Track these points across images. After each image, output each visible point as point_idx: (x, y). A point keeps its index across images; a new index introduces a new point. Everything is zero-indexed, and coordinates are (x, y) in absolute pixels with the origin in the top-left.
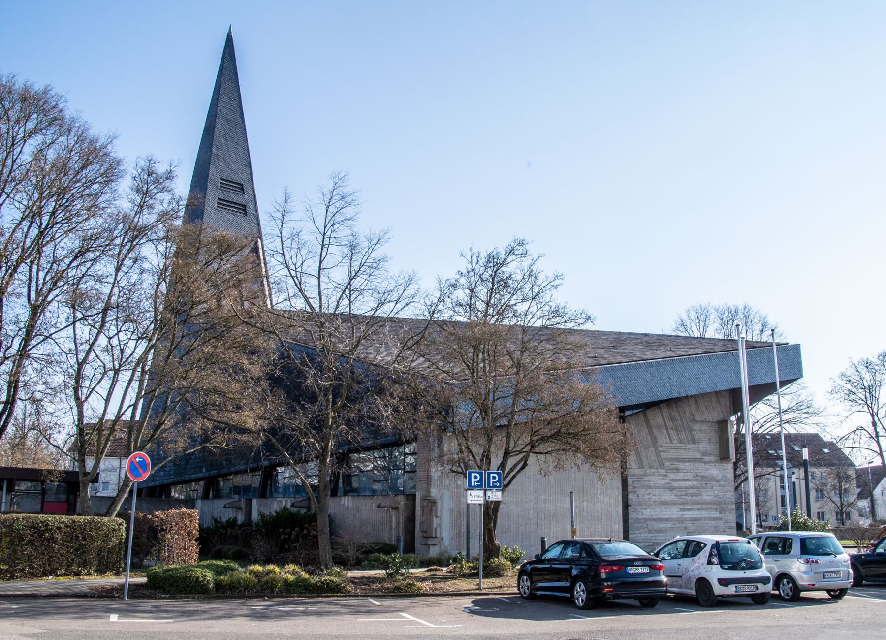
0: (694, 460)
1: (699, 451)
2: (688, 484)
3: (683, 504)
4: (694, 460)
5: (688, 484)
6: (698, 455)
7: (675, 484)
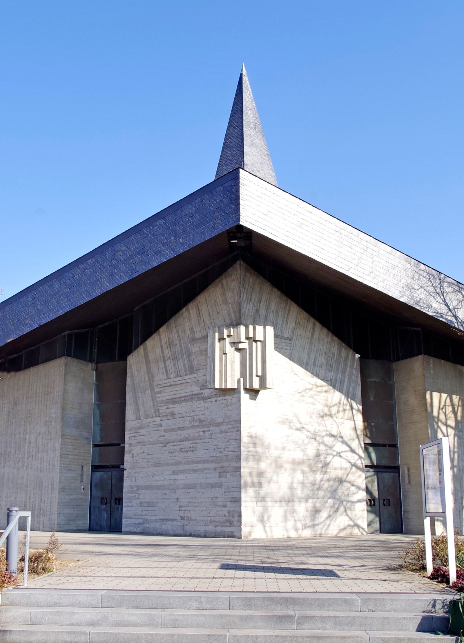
0: (193, 397)
1: (197, 383)
2: (184, 434)
3: (177, 463)
4: (193, 397)
5: (184, 434)
6: (196, 389)
7: (169, 436)
